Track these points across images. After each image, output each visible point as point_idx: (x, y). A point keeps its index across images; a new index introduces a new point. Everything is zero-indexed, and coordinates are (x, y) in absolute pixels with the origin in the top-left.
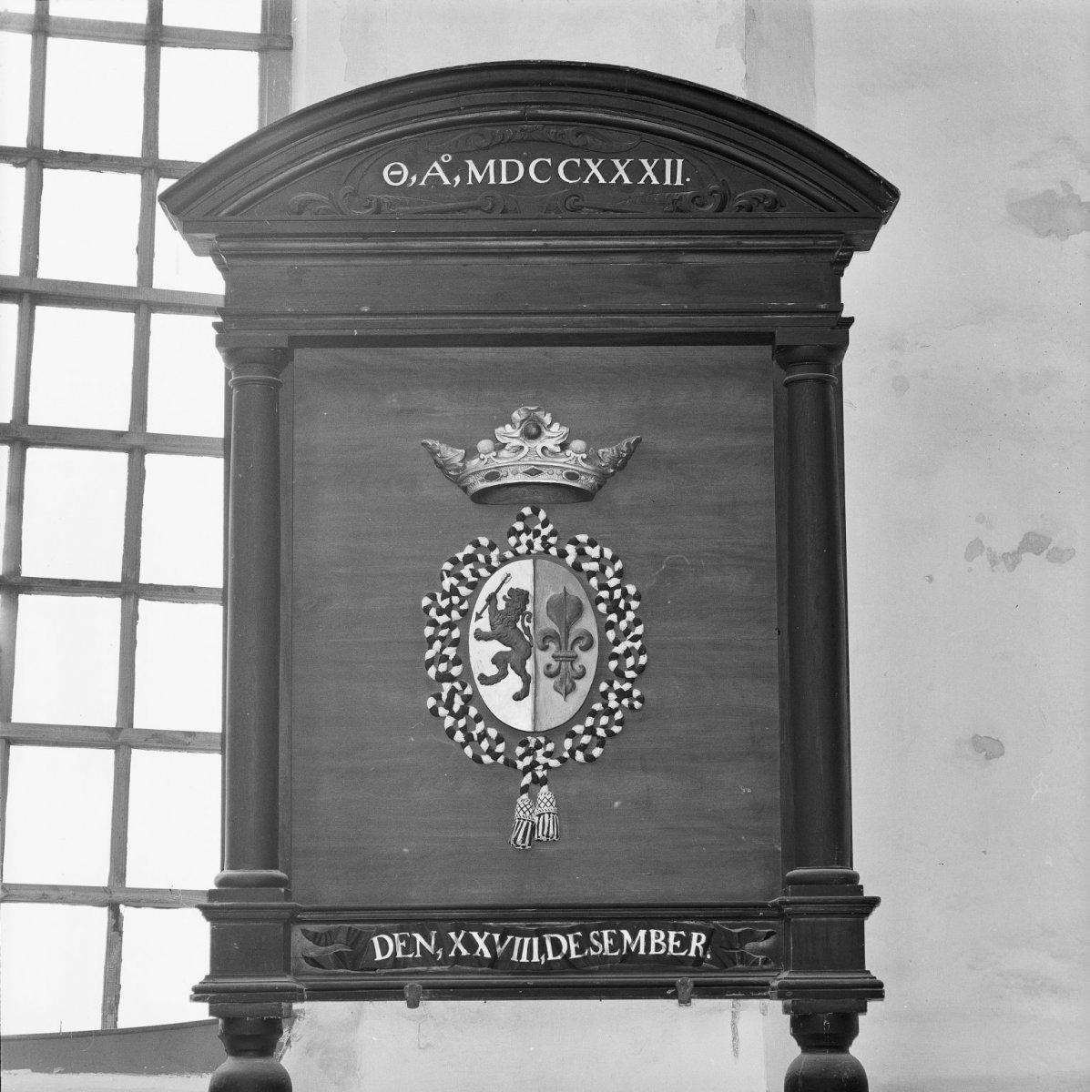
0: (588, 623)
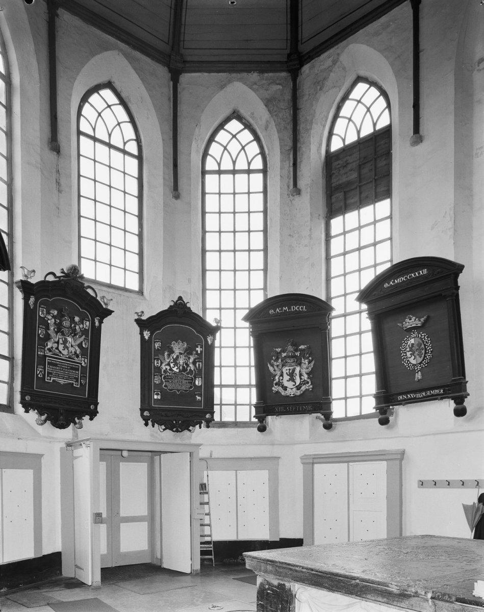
0: (423, 346)
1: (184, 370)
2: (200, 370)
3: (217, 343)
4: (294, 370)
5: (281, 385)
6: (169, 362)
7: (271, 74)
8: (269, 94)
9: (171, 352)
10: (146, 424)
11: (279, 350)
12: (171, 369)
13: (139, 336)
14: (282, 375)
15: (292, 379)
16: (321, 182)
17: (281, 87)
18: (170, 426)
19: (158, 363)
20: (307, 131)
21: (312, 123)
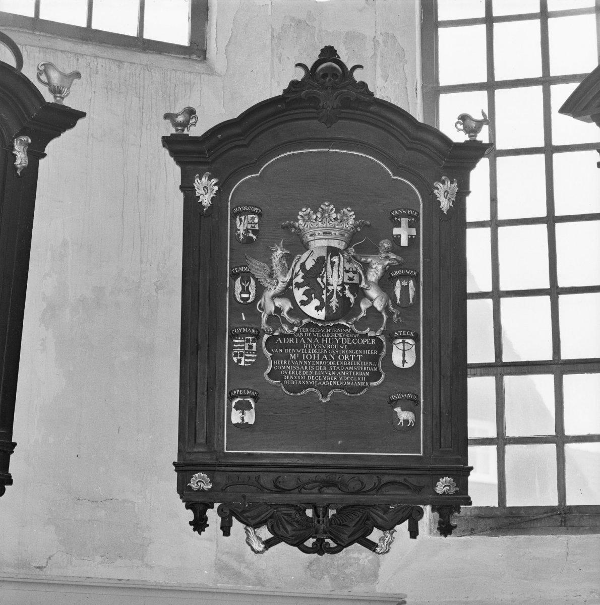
1: (347, 309)
2: (408, 309)
3: (476, 207)
6: (290, 283)
9: (298, 245)
10: (199, 524)
12: (296, 311)
13: (181, 195)
18: (290, 528)
19: (245, 290)
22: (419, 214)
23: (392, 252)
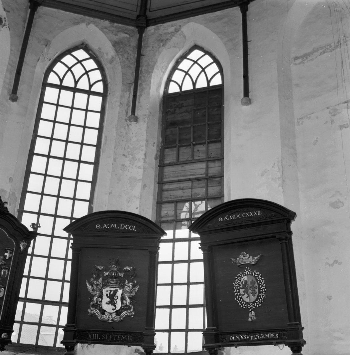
0: (256, 285)
4: (115, 292)
5: (98, 308)
7: (120, 25)
8: (117, 39)
11: (101, 268)
14: (101, 296)
15: (112, 302)
16: (157, 116)
17: (128, 36)
20: (150, 73)
21: (153, 68)
22: (13, 250)
23: (3, 260)
